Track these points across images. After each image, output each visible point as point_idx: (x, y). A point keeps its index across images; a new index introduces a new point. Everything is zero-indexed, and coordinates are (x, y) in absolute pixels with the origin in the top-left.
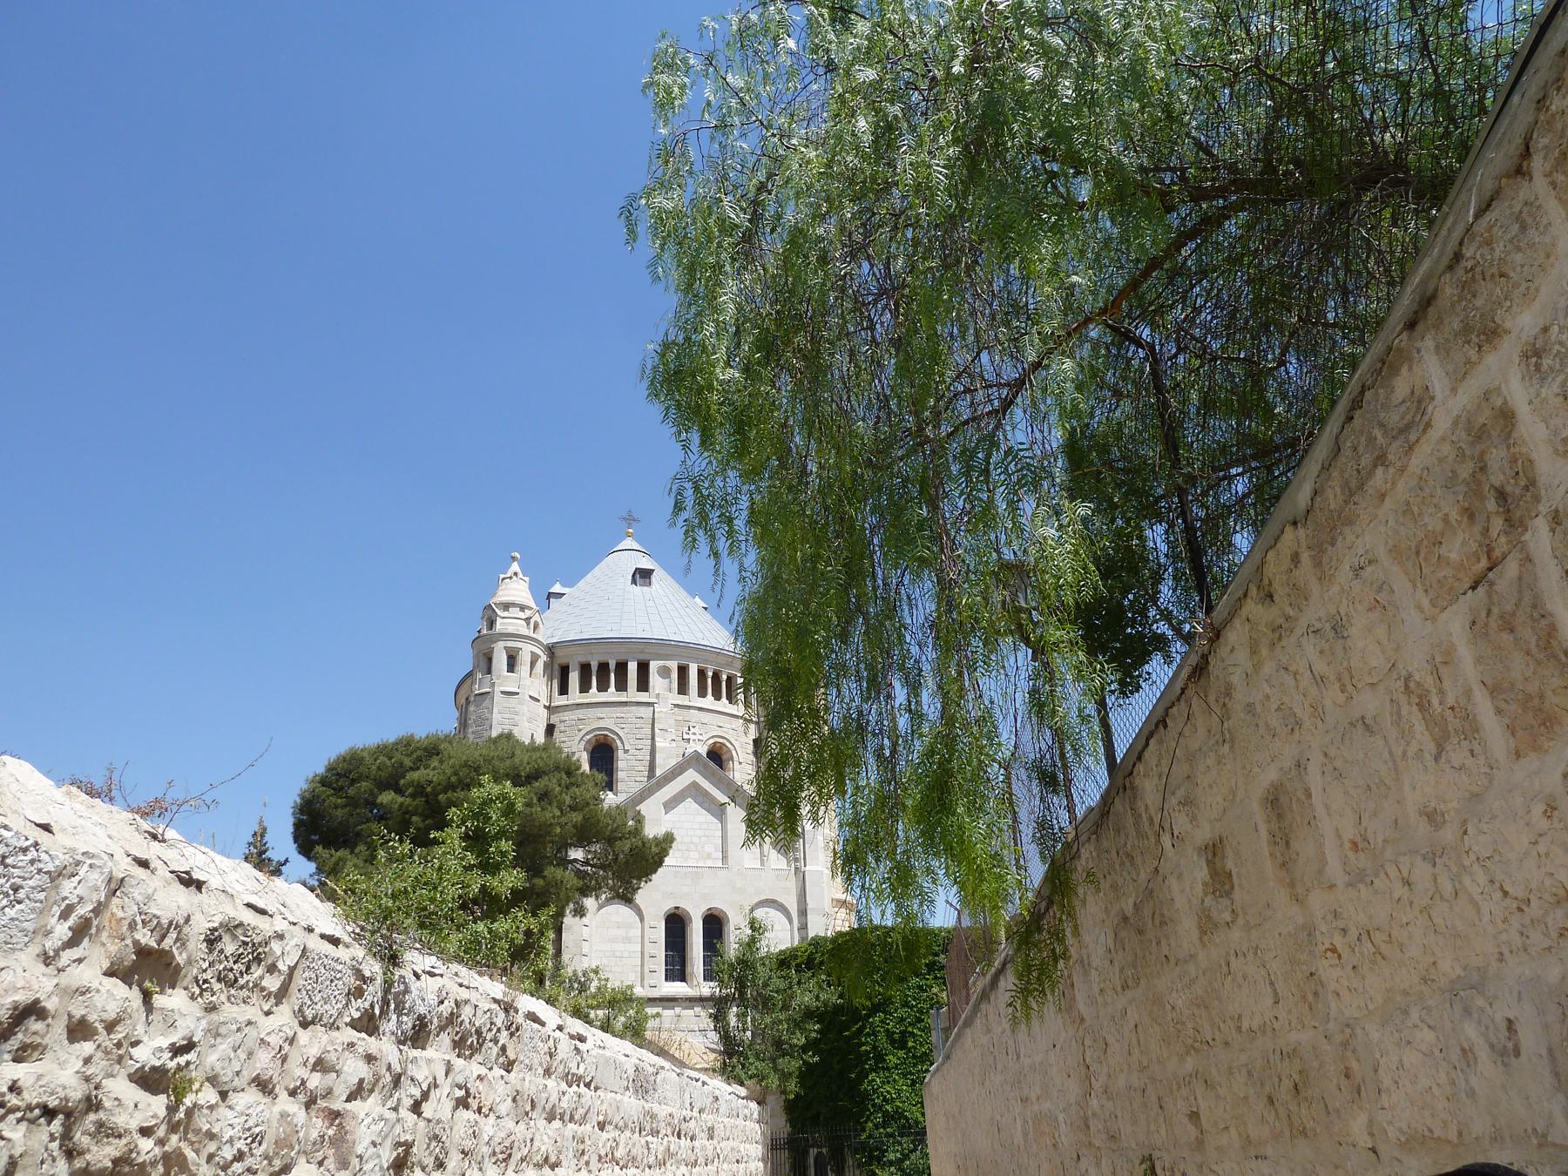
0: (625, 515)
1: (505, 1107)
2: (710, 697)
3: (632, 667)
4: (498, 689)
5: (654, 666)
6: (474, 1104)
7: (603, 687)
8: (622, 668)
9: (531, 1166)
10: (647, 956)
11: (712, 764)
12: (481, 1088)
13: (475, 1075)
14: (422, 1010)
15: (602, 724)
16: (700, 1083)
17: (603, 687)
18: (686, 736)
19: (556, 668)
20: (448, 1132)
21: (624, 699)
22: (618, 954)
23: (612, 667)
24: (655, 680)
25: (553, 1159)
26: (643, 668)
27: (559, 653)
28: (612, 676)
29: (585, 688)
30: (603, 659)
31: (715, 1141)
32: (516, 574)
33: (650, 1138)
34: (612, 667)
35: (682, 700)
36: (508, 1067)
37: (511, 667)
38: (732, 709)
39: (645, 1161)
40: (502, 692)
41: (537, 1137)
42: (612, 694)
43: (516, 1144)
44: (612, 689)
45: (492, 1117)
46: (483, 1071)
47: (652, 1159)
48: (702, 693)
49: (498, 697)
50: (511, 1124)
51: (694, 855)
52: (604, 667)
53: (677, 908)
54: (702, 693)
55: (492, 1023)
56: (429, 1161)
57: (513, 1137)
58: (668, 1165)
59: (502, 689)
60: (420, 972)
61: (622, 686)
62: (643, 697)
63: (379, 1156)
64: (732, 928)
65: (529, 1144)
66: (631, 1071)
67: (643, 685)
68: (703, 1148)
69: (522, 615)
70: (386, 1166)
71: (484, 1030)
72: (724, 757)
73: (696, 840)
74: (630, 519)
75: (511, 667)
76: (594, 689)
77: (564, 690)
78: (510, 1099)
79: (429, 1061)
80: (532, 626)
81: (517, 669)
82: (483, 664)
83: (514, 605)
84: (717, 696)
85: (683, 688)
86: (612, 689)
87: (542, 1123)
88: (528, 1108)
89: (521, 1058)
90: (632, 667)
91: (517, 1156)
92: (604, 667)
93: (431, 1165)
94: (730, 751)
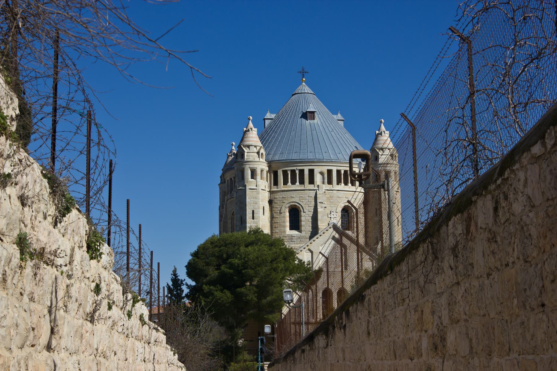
0: (301, 70)
3: (306, 173)
4: (247, 188)
5: (317, 170)
7: (293, 183)
15: (293, 200)
21: (303, 188)
24: (318, 178)
26: (311, 172)
27: (273, 165)
35: (329, 187)
38: (353, 188)
42: (297, 186)
44: (298, 183)
48: (339, 182)
49: (248, 191)
54: (339, 182)
59: (250, 187)
61: (302, 182)
62: (311, 187)
67: (312, 181)
74: (303, 73)
76: (289, 183)
77: (276, 183)
84: (346, 184)
86: (298, 183)
90: (306, 173)
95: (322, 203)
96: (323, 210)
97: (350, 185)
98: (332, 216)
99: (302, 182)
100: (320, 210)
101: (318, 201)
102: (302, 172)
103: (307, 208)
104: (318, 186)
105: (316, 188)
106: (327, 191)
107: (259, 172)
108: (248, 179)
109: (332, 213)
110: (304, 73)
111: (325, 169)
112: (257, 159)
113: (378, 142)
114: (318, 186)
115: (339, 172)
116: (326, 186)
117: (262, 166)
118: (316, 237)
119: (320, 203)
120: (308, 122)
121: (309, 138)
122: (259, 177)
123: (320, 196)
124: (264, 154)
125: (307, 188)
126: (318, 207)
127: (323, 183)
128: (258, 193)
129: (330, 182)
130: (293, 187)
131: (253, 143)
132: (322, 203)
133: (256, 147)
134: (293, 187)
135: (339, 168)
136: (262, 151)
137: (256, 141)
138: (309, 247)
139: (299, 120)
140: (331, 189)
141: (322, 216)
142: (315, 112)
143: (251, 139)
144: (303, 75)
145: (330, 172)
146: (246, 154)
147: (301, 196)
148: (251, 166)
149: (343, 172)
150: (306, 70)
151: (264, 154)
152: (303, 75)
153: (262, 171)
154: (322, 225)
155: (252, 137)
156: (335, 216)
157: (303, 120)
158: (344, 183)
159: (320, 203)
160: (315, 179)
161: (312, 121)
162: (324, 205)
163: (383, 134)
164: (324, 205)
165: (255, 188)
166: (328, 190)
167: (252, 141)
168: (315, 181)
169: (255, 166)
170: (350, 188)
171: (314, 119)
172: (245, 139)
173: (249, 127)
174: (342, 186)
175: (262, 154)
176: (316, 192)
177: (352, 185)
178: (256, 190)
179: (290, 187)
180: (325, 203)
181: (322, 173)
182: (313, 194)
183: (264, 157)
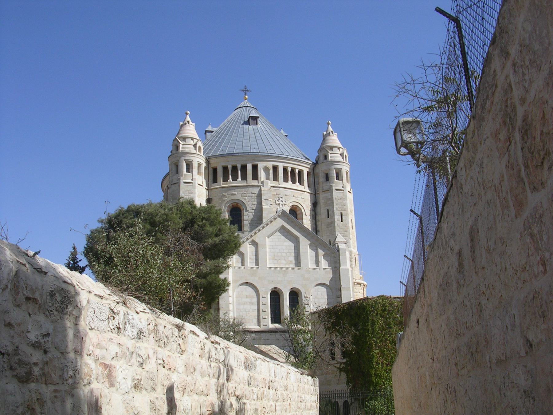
0: (243, 89)
1: (181, 369)
2: (290, 182)
3: (249, 167)
4: (181, 181)
6: (167, 367)
7: (235, 178)
8: (244, 168)
9: (195, 394)
10: (261, 311)
11: (291, 216)
12: (170, 361)
13: (167, 355)
14: (141, 326)
15: (235, 197)
16: (279, 366)
17: (235, 178)
18: (277, 202)
19: (211, 169)
20: (156, 377)
21: (245, 184)
22: (247, 310)
23: (239, 167)
24: (262, 175)
25: (205, 392)
27: (212, 161)
28: (240, 172)
29: (226, 179)
30: (234, 164)
31: (288, 392)
32: (188, 122)
33: (253, 388)
34: (239, 167)
35: (275, 184)
36: (182, 352)
38: (301, 188)
39: (251, 397)
40: (185, 183)
41: (197, 383)
42: (239, 182)
43: (188, 385)
44: (240, 179)
45: (175, 372)
46: (170, 354)
47: (255, 397)
48: (286, 180)
49: (182, 185)
50: (185, 377)
51: (284, 262)
52: (235, 168)
53: (275, 288)
54: (286, 180)
55: (173, 334)
56: (149, 388)
57: (185, 382)
58: (264, 400)
59: (184, 181)
60: (139, 311)
61: (244, 178)
62: (255, 183)
63: (127, 383)
64: (303, 297)
65: (194, 385)
66: (243, 359)
67: (255, 177)
68: (282, 394)
70: (130, 387)
71: (170, 337)
72: (298, 213)
73: (284, 255)
74: (246, 91)
75: (188, 170)
77: (215, 181)
78: (183, 366)
79: (146, 348)
82: (174, 169)
84: (294, 182)
85: (276, 178)
86: (240, 179)
87: (199, 378)
88: (193, 371)
89: (188, 349)
90: (249, 167)
91: (188, 390)
92: (235, 168)
93: (150, 389)
94: (300, 209)
95: (268, 200)
96: (269, 207)
97: (297, 183)
98: (281, 203)
99: (244, 178)
100: (265, 206)
101: (263, 198)
103: (250, 206)
104: (262, 182)
105: (260, 184)
106: (272, 188)
107: (195, 165)
108: (183, 171)
109: (281, 199)
110: (247, 92)
111: (270, 165)
112: (194, 151)
113: (327, 142)
114: (262, 182)
115: (285, 169)
116: (271, 183)
117: (199, 160)
118: (262, 225)
119: (265, 199)
120: (251, 127)
121: (253, 139)
122: (195, 170)
123: (265, 192)
124: (202, 148)
125: (250, 184)
126: (263, 204)
127: (268, 178)
128: (194, 188)
129: (276, 178)
130: (235, 184)
131: (190, 135)
132: (268, 200)
133: (192, 139)
134: (235, 184)
135: (286, 165)
136: (200, 144)
137: (193, 134)
138: (253, 238)
139: (241, 126)
140: (277, 186)
141: (267, 214)
142: (258, 117)
143: (187, 131)
144: (246, 93)
145: (275, 168)
146: (181, 146)
147: (243, 192)
148: (187, 158)
149: (289, 169)
151: (202, 148)
152: (246, 93)
153: (199, 165)
154: (267, 216)
155: (188, 130)
156: (284, 203)
157: (246, 126)
158: (291, 181)
159: (265, 199)
160: (259, 174)
161: (255, 127)
162: (269, 203)
163: (331, 134)
164: (269, 203)
165: (191, 181)
166: (273, 187)
167: (188, 133)
168: (259, 176)
169: (191, 158)
170: (298, 186)
171: (257, 124)
172: (181, 132)
173: (186, 122)
174: (289, 184)
175: (200, 148)
176: (260, 190)
177: (300, 185)
178: (191, 184)
179: (231, 183)
180: (271, 200)
181: (266, 169)
182: (256, 190)
183: (202, 151)
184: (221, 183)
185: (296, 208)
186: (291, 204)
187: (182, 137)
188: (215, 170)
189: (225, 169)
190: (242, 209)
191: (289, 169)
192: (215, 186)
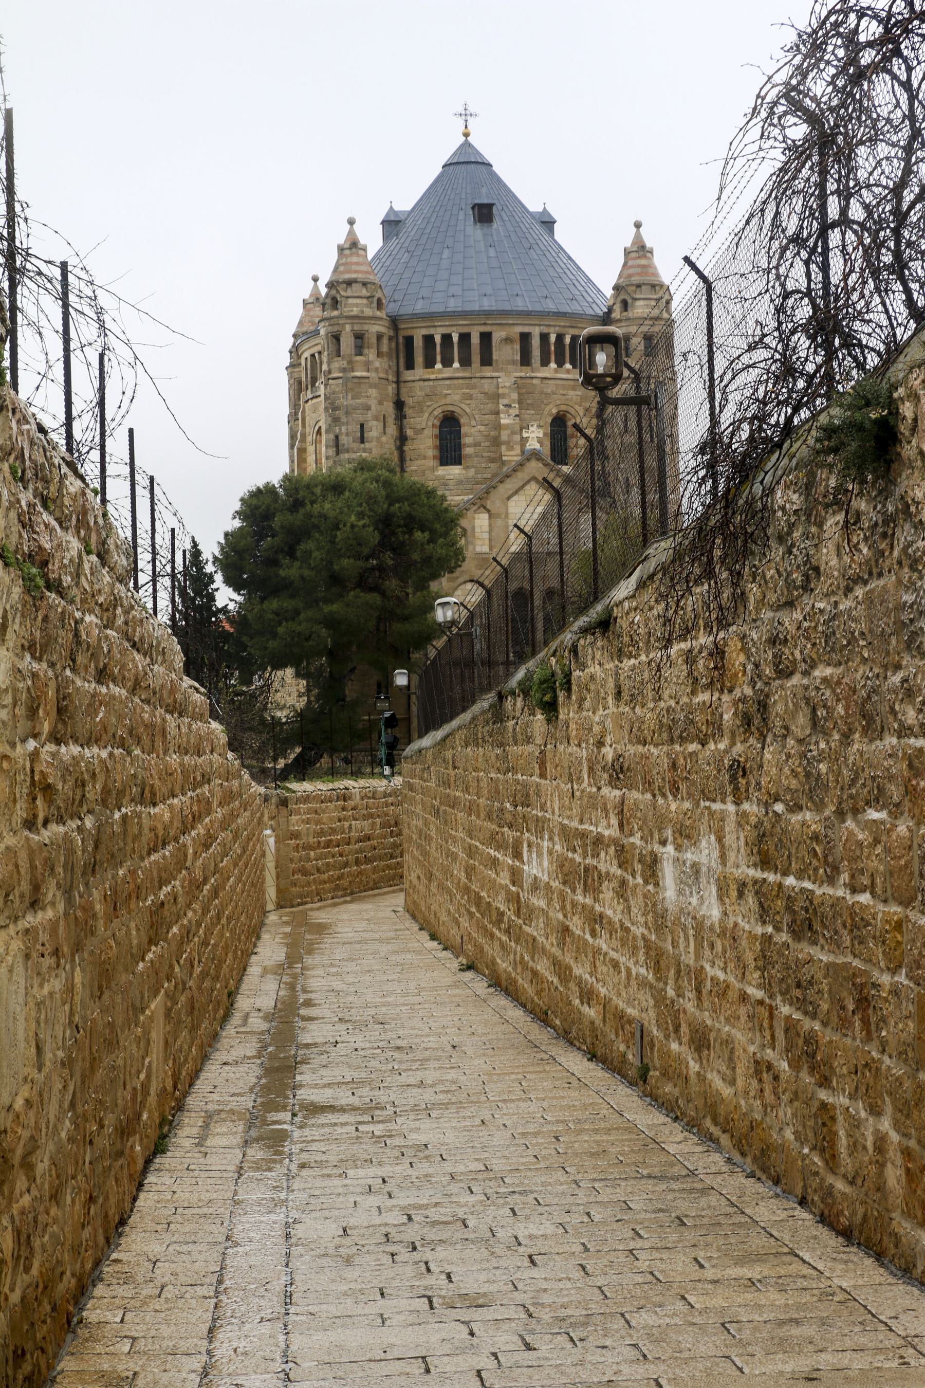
2: (553, 365)
3: (475, 340)
5: (498, 335)
7: (447, 363)
15: (448, 400)
17: (447, 363)
19: (401, 340)
21: (467, 375)
26: (486, 338)
29: (429, 363)
37: (359, 350)
44: (456, 365)
48: (545, 362)
52: (447, 338)
62: (488, 371)
67: (487, 360)
69: (364, 292)
76: (439, 366)
77: (410, 366)
80: (375, 305)
81: (366, 351)
83: (355, 281)
85: (525, 360)
86: (456, 365)
90: (475, 340)
99: (466, 362)
102: (465, 338)
115: (544, 337)
130: (448, 372)
145: (525, 338)
150: (471, 109)
153: (379, 337)
159: (506, 406)
170: (568, 371)
184: (419, 372)
185: (564, 415)
186: (554, 411)
187: (344, 282)
188: (409, 341)
189: (429, 340)
190: (462, 421)
191: (553, 338)
192: (408, 375)
